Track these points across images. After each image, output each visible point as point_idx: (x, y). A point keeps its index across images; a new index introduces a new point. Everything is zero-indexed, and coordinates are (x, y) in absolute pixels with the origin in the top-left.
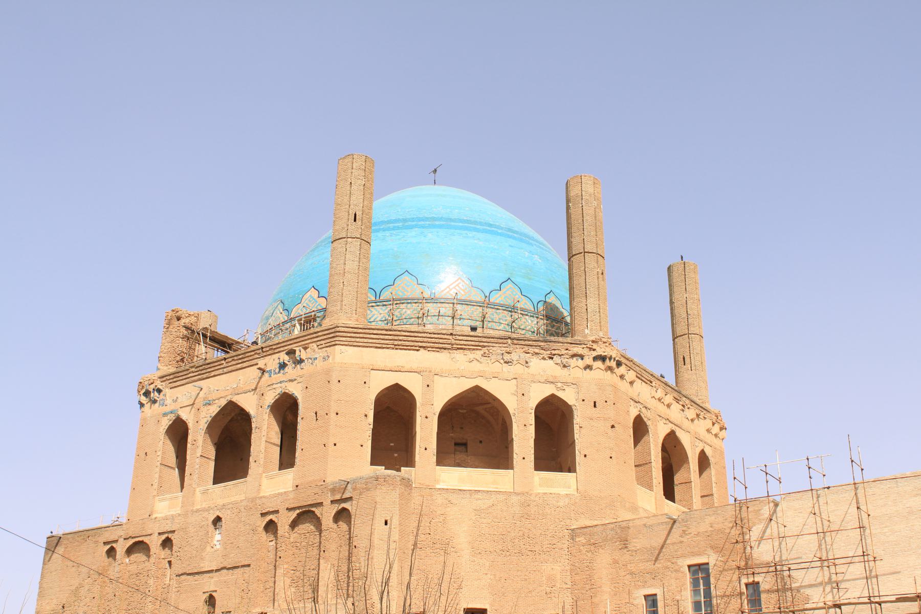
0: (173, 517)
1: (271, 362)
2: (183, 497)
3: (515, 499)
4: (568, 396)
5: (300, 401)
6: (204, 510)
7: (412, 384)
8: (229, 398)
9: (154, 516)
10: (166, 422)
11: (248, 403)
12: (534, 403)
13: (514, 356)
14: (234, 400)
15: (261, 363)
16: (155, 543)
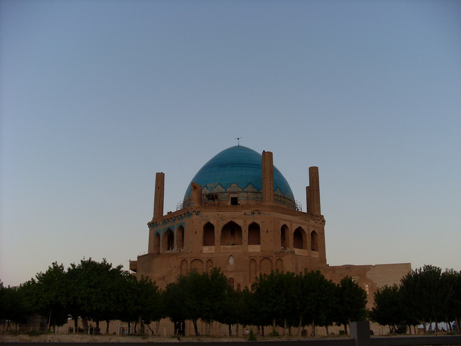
0: (212, 253)
1: (248, 212)
2: (215, 248)
3: (308, 258)
4: (317, 231)
5: (261, 226)
6: (225, 253)
7: (288, 224)
8: (231, 220)
9: (203, 252)
10: (204, 223)
11: (239, 222)
12: (311, 232)
13: (307, 219)
14: (233, 220)
15: (243, 212)
16: (205, 261)
